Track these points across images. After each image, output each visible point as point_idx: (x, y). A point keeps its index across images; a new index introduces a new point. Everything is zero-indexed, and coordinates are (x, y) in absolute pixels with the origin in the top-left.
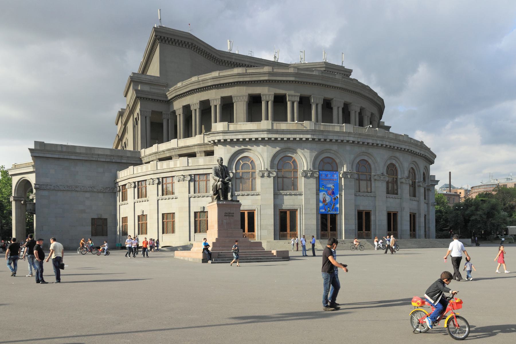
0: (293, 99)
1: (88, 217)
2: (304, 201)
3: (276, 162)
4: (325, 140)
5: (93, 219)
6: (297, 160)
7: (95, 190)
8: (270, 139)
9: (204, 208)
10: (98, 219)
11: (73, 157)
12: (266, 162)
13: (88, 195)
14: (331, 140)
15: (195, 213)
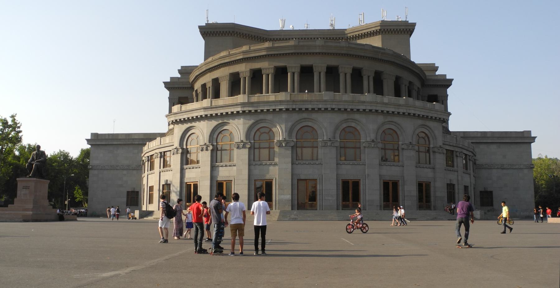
0: (268, 72)
1: (124, 190)
2: (279, 172)
3: (215, 136)
4: (256, 111)
5: (128, 192)
6: (233, 132)
7: (131, 168)
8: (206, 115)
9: (167, 180)
10: (132, 192)
11: (115, 143)
12: (205, 136)
13: (125, 172)
14: (262, 111)
15: (163, 185)
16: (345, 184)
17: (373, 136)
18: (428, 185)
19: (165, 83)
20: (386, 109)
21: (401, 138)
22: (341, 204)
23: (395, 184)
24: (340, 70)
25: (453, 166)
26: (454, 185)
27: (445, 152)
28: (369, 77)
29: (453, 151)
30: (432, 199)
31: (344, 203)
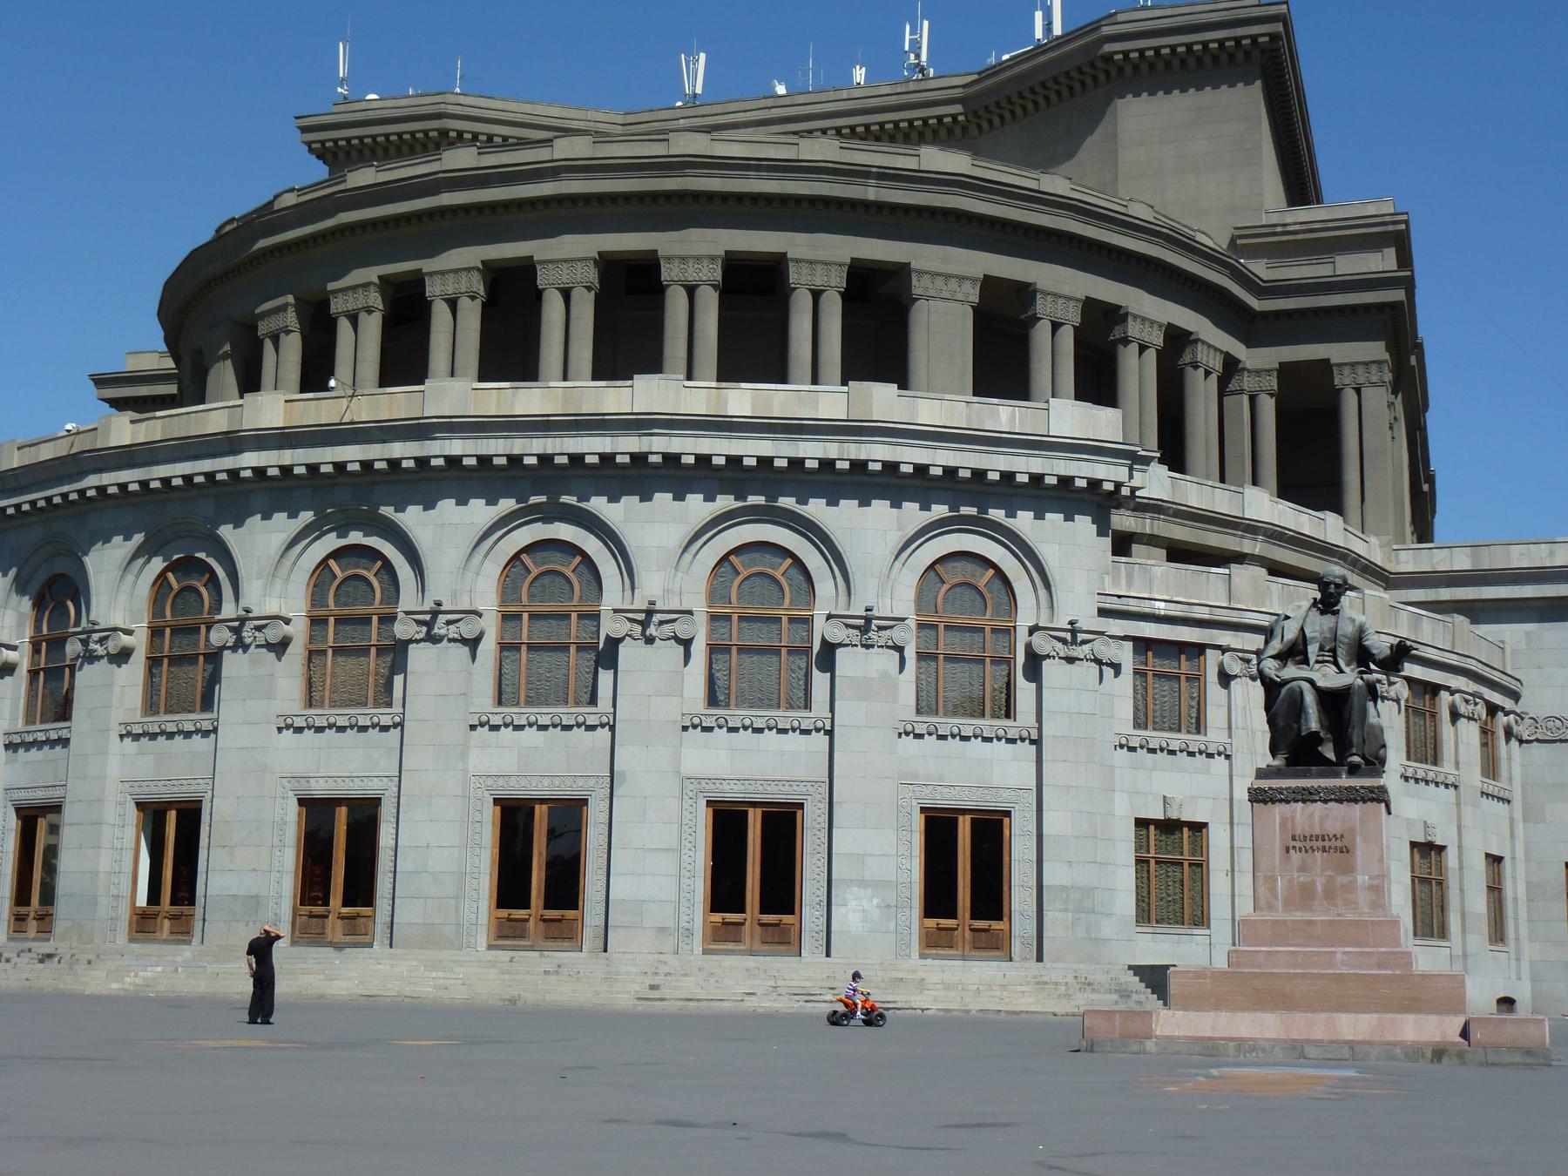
16: (514, 817)
17: (653, 586)
18: (990, 829)
19: (100, 381)
20: (719, 447)
21: (825, 585)
22: (484, 918)
23: (782, 823)
24: (668, 273)
25: (1199, 726)
26: (1199, 828)
27: (1125, 655)
28: (816, 295)
29: (1200, 649)
30: (1020, 897)
31: (504, 913)
